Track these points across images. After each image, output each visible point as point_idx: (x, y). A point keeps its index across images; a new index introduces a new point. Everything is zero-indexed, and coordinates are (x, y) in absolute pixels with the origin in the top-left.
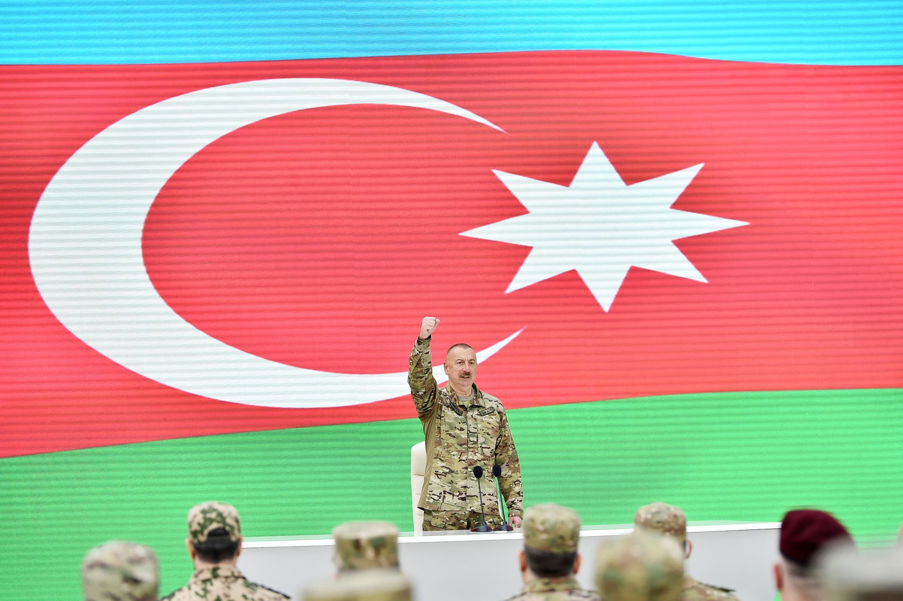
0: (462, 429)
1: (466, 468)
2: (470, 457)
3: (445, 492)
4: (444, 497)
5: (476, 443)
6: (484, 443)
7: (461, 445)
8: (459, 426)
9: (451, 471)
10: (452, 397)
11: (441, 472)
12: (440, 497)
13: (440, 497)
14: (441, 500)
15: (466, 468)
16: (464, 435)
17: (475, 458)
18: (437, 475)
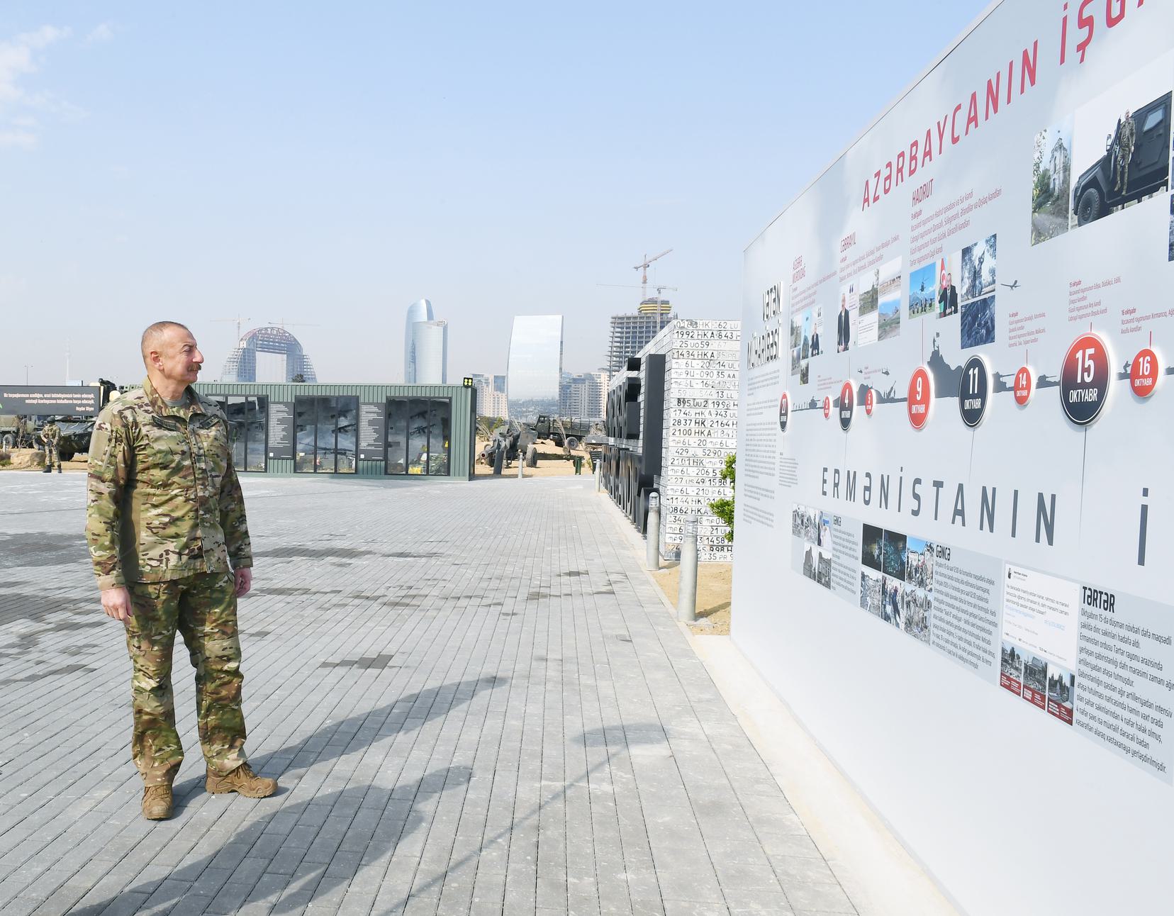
0: (183, 453)
1: (197, 511)
2: (200, 494)
3: (167, 552)
4: (168, 560)
5: (204, 471)
6: (213, 470)
7: (184, 477)
8: (179, 448)
9: (174, 521)
10: (153, 403)
11: (156, 523)
12: (161, 561)
13: (161, 561)
14: (163, 565)
16: (187, 463)
17: (207, 494)
18: (150, 528)
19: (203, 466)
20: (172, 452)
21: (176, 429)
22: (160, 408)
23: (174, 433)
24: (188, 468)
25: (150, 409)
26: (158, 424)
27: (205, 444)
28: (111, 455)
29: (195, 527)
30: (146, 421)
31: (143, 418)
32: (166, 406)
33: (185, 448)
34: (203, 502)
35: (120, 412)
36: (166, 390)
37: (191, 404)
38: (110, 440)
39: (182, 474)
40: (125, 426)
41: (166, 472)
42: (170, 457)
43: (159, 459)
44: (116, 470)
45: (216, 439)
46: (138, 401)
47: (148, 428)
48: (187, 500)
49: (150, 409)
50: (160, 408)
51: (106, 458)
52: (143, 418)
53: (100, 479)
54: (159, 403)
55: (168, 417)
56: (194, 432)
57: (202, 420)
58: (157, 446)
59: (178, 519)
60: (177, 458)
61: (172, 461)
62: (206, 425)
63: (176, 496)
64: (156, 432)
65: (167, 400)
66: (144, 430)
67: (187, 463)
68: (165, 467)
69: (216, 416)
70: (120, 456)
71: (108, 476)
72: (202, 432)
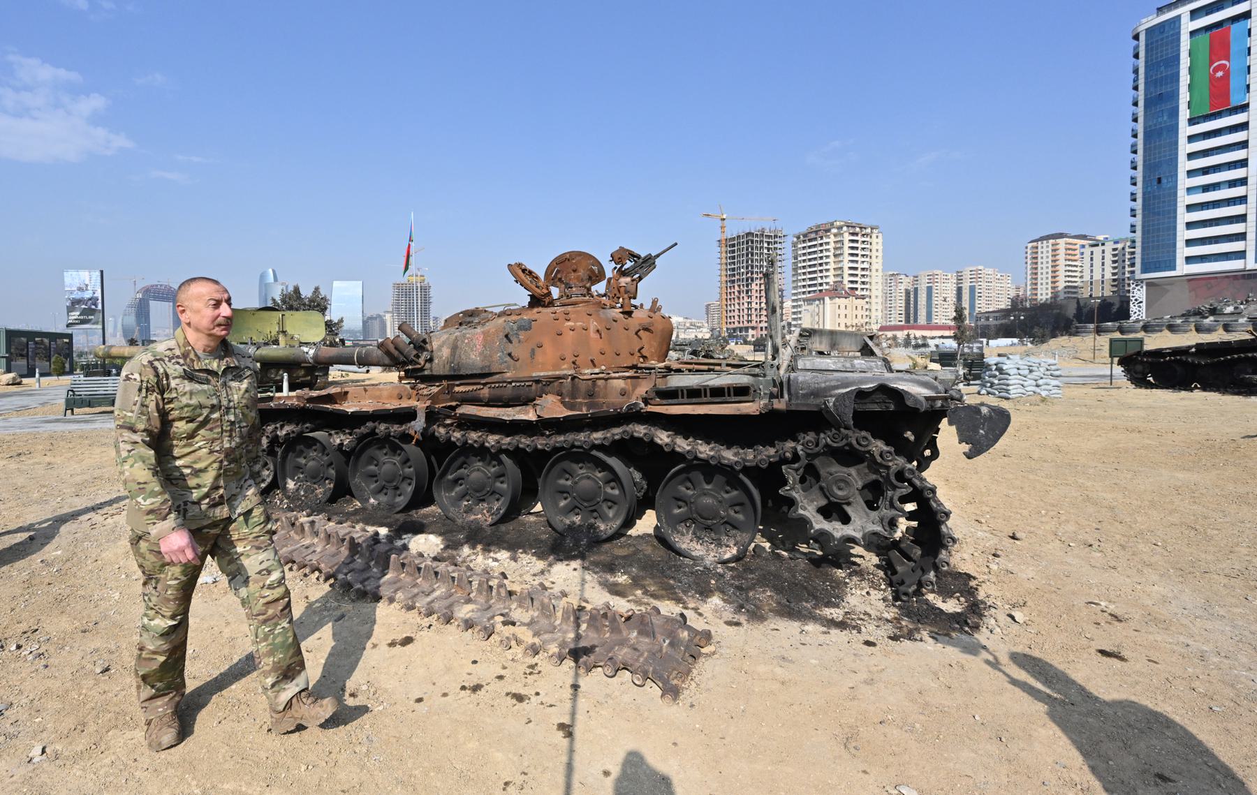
0: (213, 406)
2: (227, 445)
5: (232, 423)
7: (211, 430)
10: (185, 356)
15: (221, 462)
17: (233, 444)
19: (232, 418)
20: (201, 406)
21: (208, 382)
22: (192, 361)
23: (205, 387)
24: (216, 420)
25: (181, 361)
26: (189, 376)
27: (236, 397)
28: (143, 405)
29: (217, 478)
30: (177, 374)
31: (174, 369)
32: (199, 358)
33: (215, 401)
34: (229, 453)
35: (151, 363)
36: (199, 342)
37: (225, 356)
38: (140, 390)
39: (208, 427)
40: (157, 375)
41: (192, 426)
42: (199, 410)
43: (186, 413)
44: (149, 419)
45: (247, 391)
46: (168, 353)
47: (177, 381)
48: (211, 452)
49: (181, 361)
50: (192, 361)
51: (136, 408)
52: (174, 369)
53: (133, 430)
54: (192, 356)
55: (200, 371)
56: (225, 384)
57: (234, 373)
58: (185, 400)
59: (201, 471)
60: (205, 412)
61: (200, 415)
62: (239, 377)
63: (200, 448)
64: (188, 386)
65: (200, 353)
66: (173, 383)
67: (216, 415)
68: (191, 421)
69: (249, 368)
70: (152, 406)
71: (141, 426)
72: (234, 384)
